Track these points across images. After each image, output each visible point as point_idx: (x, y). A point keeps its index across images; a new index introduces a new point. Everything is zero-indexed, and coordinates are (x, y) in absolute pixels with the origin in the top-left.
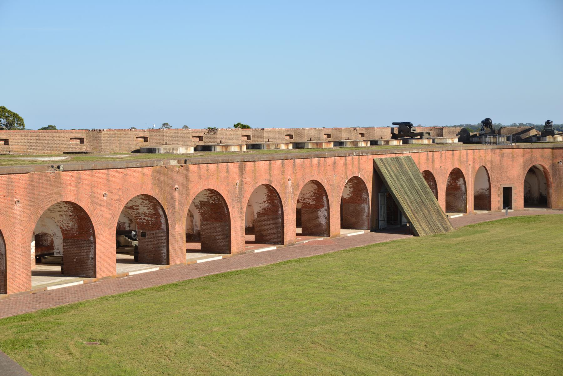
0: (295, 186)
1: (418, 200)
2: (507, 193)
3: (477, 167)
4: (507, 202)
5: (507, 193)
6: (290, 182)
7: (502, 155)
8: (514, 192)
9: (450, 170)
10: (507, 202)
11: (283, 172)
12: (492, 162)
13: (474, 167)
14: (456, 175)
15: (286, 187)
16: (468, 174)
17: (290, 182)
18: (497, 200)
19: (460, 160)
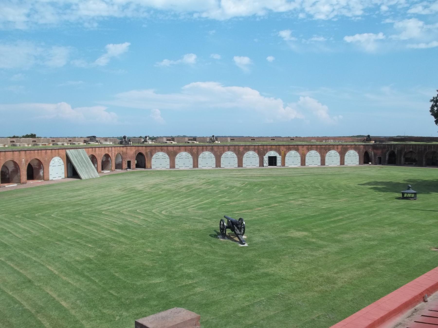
0: (26, 161)
1: (85, 165)
2: (129, 163)
3: (116, 153)
4: (129, 166)
5: (129, 163)
6: (23, 160)
7: (127, 149)
8: (132, 162)
9: (104, 154)
10: (129, 166)
11: (20, 155)
12: (123, 151)
13: (115, 153)
14: (107, 156)
15: (22, 161)
16: (112, 156)
17: (23, 160)
18: (125, 165)
19: (108, 151)
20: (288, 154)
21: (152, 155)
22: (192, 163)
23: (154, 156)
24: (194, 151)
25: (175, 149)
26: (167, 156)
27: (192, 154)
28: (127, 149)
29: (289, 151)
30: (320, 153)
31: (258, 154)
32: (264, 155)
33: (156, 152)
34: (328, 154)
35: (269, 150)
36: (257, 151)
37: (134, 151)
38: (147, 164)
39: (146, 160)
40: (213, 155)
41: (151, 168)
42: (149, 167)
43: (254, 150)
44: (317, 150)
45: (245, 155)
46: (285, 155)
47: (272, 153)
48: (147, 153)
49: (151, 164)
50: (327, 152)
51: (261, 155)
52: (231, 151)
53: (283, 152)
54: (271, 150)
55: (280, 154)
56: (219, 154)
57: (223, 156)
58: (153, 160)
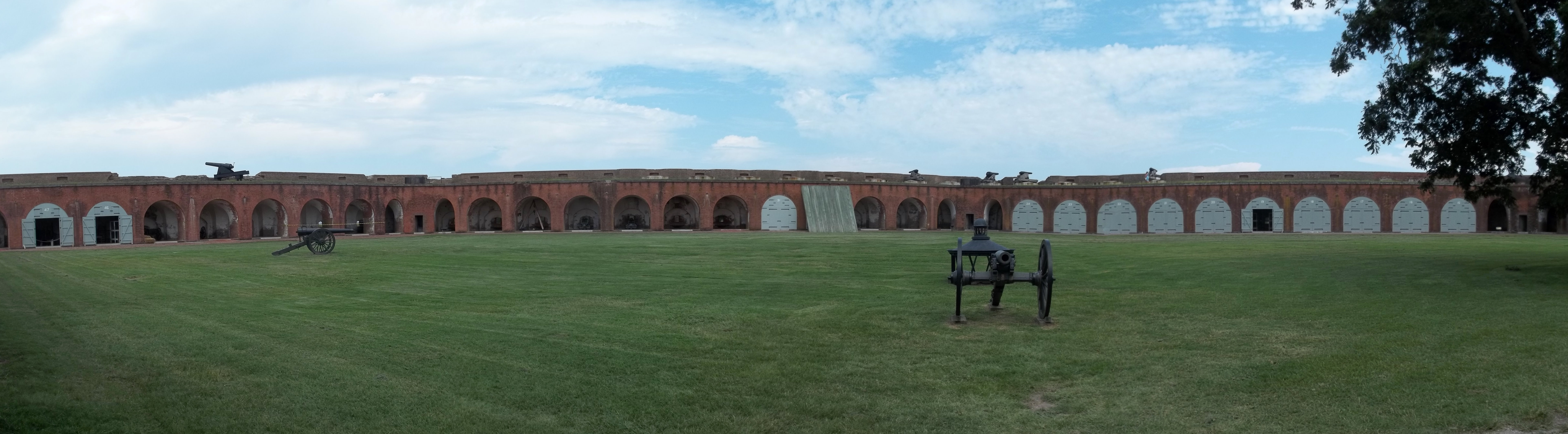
20: (1299, 205)
21: (1013, 206)
22: (1085, 223)
23: (1017, 207)
24: (1089, 198)
25: (1053, 194)
26: (1039, 208)
27: (1086, 205)
28: (966, 192)
29: (1302, 197)
30: (1379, 202)
31: (1229, 204)
32: (1244, 207)
33: (1019, 200)
34: (1398, 206)
35: (1253, 195)
36: (1226, 197)
37: (982, 196)
38: (1006, 223)
39: (1004, 214)
40: (1131, 207)
41: (1011, 228)
42: (1007, 228)
43: (1221, 196)
44: (1370, 196)
45: (1200, 207)
46: (1293, 206)
47: (1263, 203)
48: (1004, 202)
49: (1011, 223)
50: (1396, 202)
51: (1236, 207)
52: (1170, 197)
53: (1287, 201)
54: (1259, 194)
55: (1281, 205)
56: (1143, 204)
57: (1153, 208)
58: (1015, 215)
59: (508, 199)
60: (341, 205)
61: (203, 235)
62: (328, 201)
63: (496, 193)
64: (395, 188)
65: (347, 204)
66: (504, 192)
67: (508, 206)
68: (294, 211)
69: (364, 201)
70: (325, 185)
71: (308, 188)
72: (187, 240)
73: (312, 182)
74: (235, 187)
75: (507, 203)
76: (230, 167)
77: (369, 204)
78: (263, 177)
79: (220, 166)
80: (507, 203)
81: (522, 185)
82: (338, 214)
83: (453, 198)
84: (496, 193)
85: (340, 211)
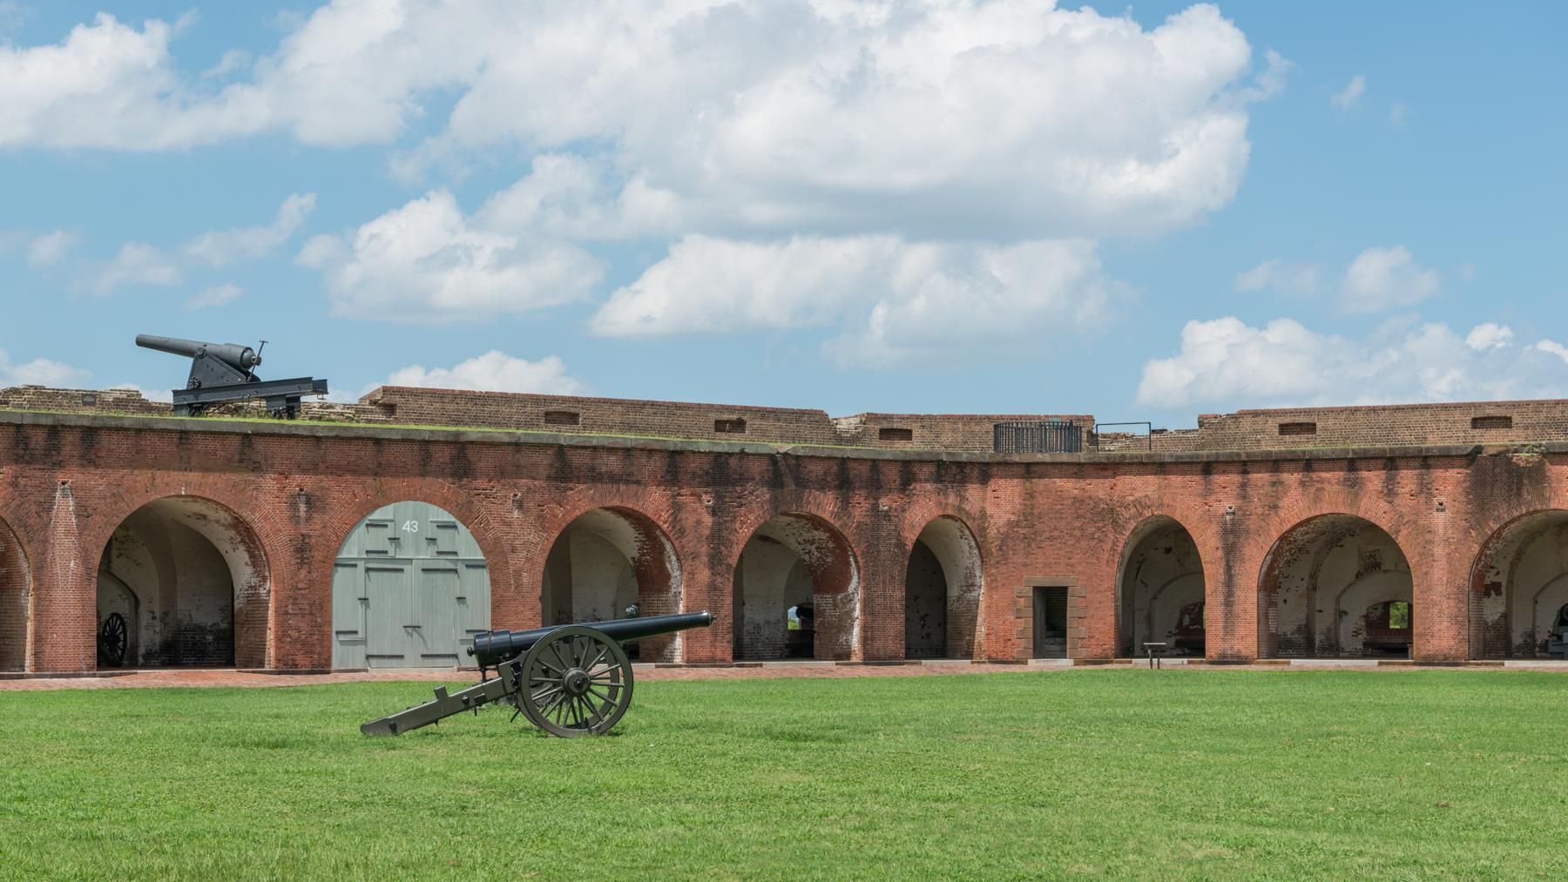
59: (1440, 520)
60: (718, 538)
61: (113, 651)
62: (663, 520)
63: (1390, 493)
64: (954, 472)
65: (744, 532)
66: (1425, 489)
67: (1439, 551)
68: (517, 560)
69: (817, 523)
70: (651, 452)
71: (578, 459)
72: (40, 670)
73: (597, 436)
74: (260, 445)
75: (1438, 536)
76: (243, 364)
77: (836, 536)
78: (390, 409)
79: (200, 356)
80: (1438, 536)
81: (1502, 457)
82: (704, 575)
83: (1197, 508)
84: (1390, 493)
85: (715, 560)
